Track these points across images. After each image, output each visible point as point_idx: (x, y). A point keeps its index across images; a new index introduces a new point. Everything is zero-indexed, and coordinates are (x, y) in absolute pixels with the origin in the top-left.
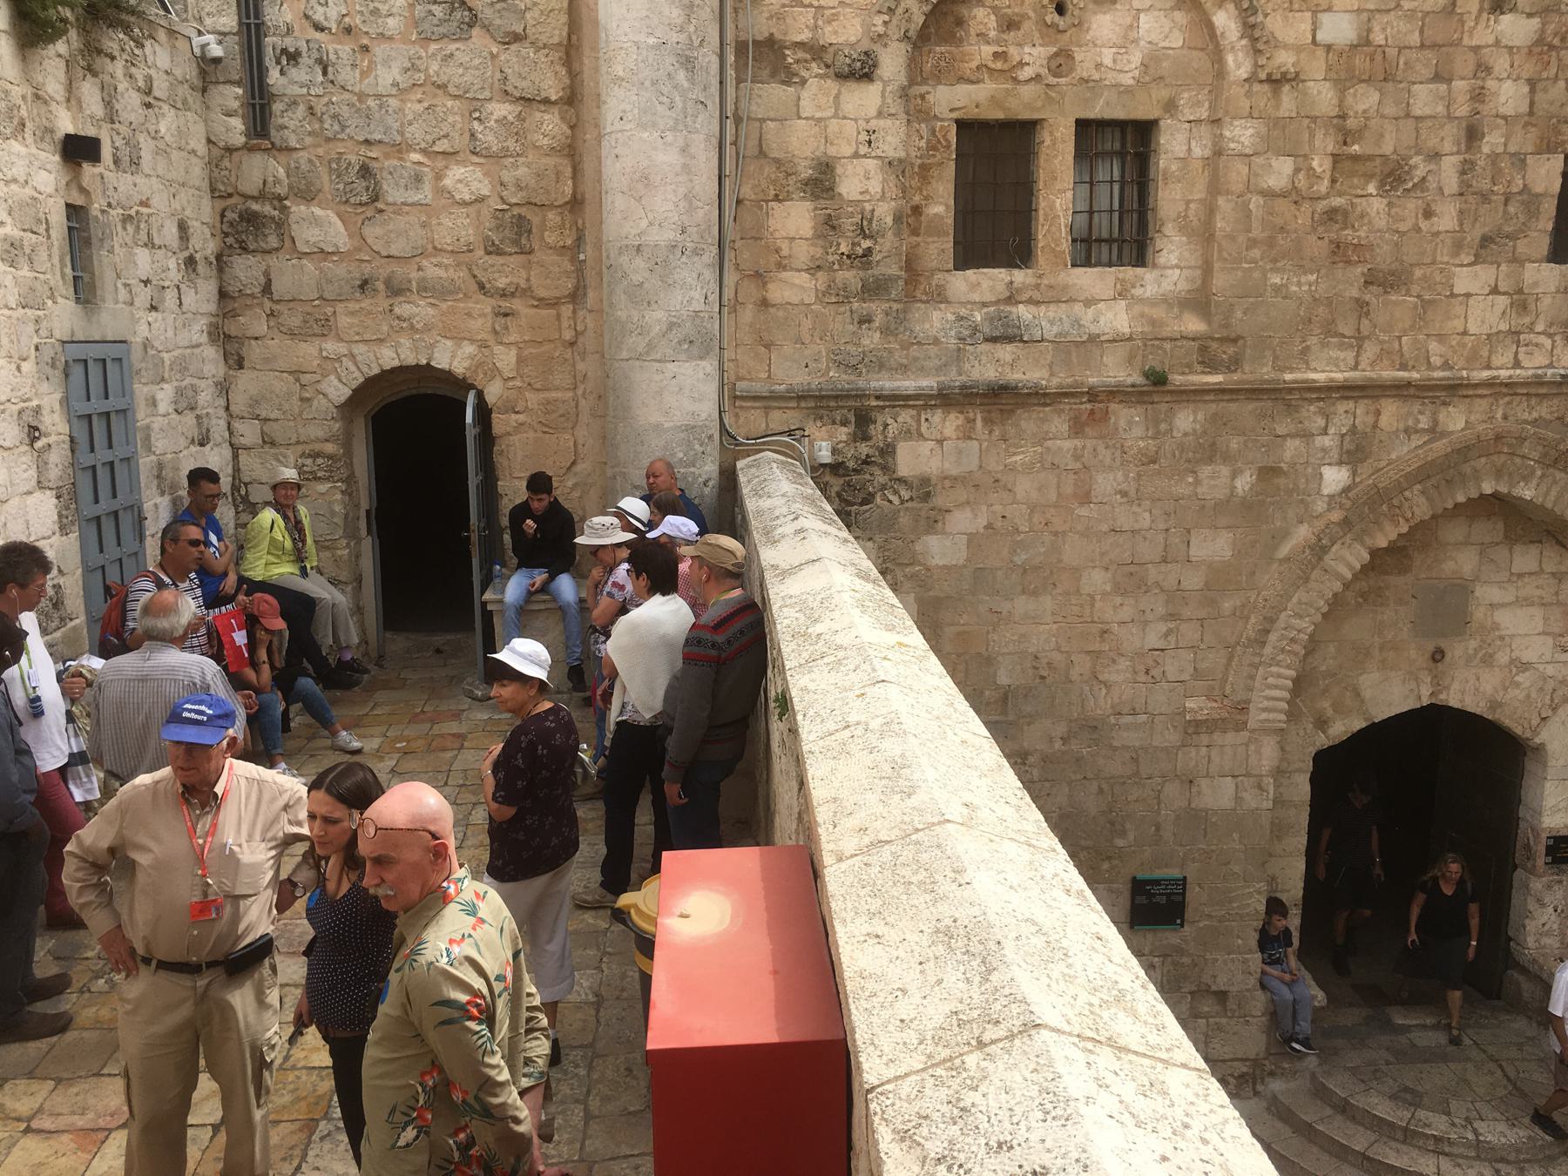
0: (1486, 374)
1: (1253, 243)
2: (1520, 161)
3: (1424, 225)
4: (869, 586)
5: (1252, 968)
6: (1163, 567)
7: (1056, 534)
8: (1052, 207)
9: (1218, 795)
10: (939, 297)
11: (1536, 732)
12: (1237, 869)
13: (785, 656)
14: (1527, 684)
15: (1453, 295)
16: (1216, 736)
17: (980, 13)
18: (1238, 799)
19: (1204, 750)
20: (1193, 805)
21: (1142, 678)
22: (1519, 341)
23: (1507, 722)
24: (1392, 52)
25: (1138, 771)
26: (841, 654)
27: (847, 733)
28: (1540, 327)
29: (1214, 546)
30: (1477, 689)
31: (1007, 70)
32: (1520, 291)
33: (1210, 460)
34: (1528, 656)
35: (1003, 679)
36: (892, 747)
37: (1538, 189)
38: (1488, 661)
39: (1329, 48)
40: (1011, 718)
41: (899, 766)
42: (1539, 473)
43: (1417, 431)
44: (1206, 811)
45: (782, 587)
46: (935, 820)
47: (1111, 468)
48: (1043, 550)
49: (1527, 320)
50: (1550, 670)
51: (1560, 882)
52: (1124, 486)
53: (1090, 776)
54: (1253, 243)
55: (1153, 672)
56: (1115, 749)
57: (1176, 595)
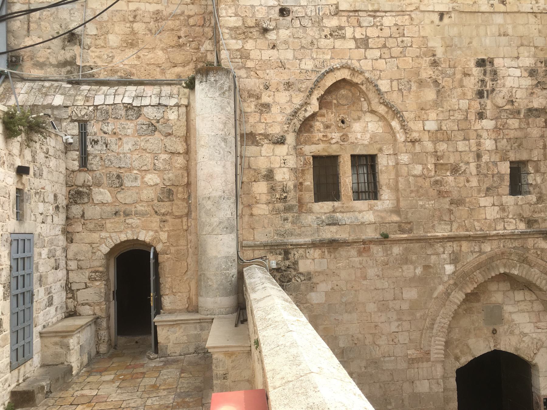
0: (495, 232)
1: (412, 191)
2: (495, 164)
3: (467, 184)
4: (288, 304)
6: (394, 302)
7: (356, 291)
8: (345, 181)
9: (423, 387)
10: (310, 211)
11: (533, 359)
13: (258, 326)
14: (527, 341)
15: (480, 207)
16: (420, 363)
17: (317, 124)
18: (430, 388)
19: (416, 370)
20: (415, 391)
21: (392, 343)
22: (504, 222)
23: (522, 356)
24: (449, 132)
25: (393, 379)
26: (277, 324)
27: (278, 348)
28: (510, 216)
29: (411, 294)
30: (510, 344)
31: (328, 141)
32: (502, 205)
33: (406, 263)
34: (526, 331)
35: (342, 345)
36: (293, 351)
37: (503, 172)
38: (512, 333)
39: (429, 131)
40: (345, 359)
41: (295, 357)
42: (518, 265)
43: (475, 252)
44: (420, 393)
45: (257, 305)
46: (308, 372)
47: (373, 267)
48: (352, 296)
49: (506, 214)
50: (534, 336)
52: (378, 273)
54: (412, 191)
56: (384, 370)
57: (400, 312)
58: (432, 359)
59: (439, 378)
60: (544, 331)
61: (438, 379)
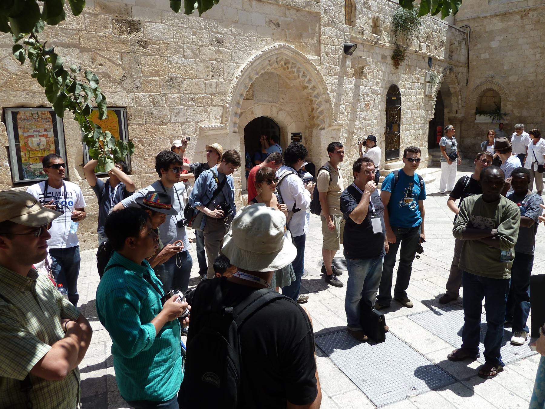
7: (517, 39)
35: (505, 68)
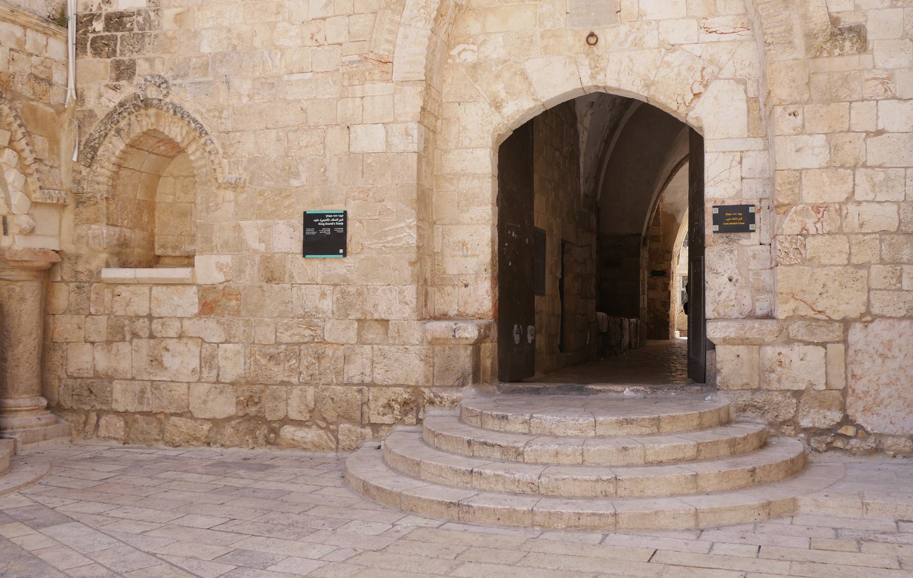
5: (408, 299)
11: (689, 107)
12: (389, 205)
16: (368, 85)
19: (358, 100)
20: (352, 150)
21: (309, 42)
35: (205, 49)
38: (638, 44)
40: (210, 78)
44: (363, 154)
50: (698, 50)
51: (731, 251)
53: (270, 126)
55: (316, 37)
58: (396, 76)
59: (409, 119)
60: (724, 38)
61: (406, 122)
